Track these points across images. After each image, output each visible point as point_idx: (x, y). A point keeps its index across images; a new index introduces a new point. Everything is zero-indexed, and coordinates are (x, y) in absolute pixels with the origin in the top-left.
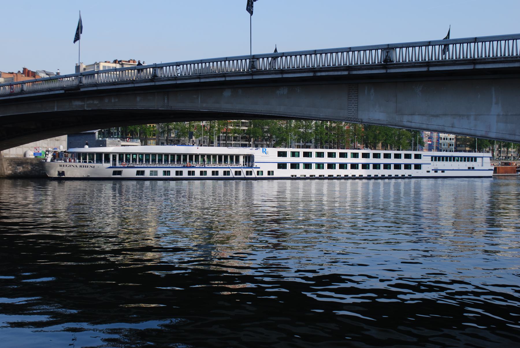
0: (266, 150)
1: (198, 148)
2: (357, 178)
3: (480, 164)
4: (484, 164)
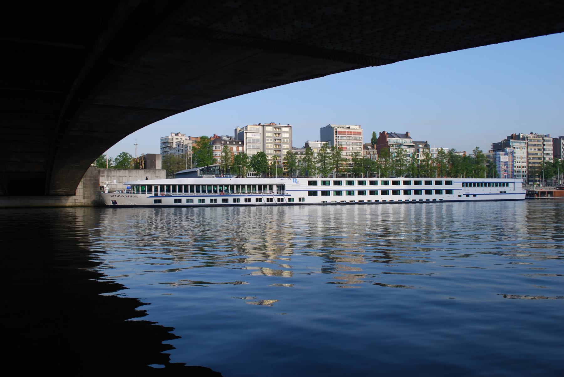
0: (296, 180)
1: (231, 179)
2: (411, 202)
3: (512, 189)
4: (515, 188)
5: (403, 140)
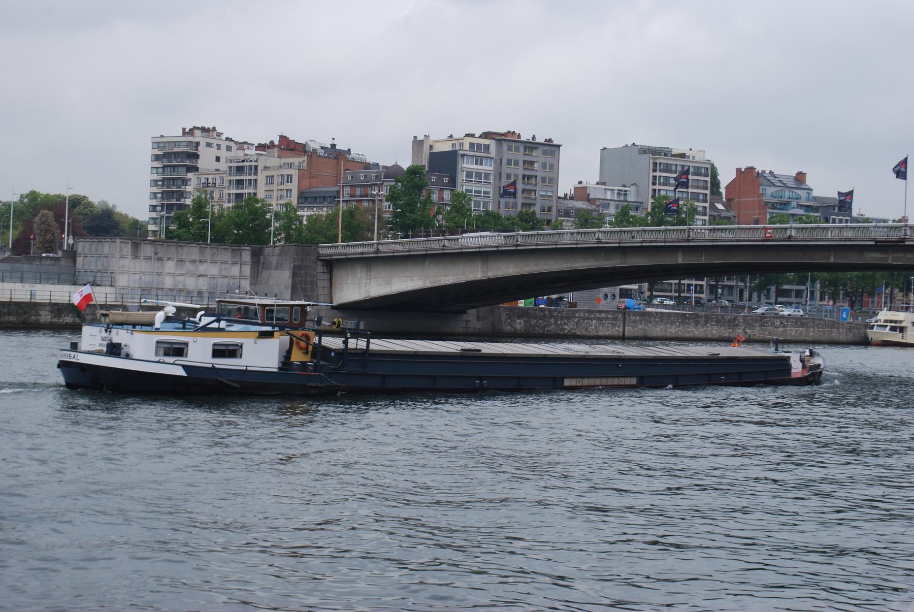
5: (794, 194)
